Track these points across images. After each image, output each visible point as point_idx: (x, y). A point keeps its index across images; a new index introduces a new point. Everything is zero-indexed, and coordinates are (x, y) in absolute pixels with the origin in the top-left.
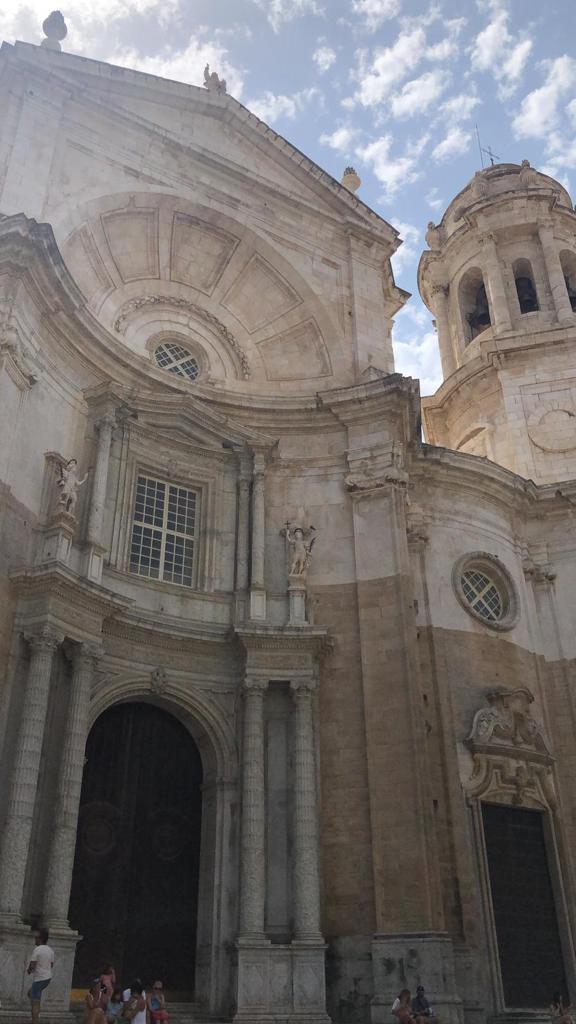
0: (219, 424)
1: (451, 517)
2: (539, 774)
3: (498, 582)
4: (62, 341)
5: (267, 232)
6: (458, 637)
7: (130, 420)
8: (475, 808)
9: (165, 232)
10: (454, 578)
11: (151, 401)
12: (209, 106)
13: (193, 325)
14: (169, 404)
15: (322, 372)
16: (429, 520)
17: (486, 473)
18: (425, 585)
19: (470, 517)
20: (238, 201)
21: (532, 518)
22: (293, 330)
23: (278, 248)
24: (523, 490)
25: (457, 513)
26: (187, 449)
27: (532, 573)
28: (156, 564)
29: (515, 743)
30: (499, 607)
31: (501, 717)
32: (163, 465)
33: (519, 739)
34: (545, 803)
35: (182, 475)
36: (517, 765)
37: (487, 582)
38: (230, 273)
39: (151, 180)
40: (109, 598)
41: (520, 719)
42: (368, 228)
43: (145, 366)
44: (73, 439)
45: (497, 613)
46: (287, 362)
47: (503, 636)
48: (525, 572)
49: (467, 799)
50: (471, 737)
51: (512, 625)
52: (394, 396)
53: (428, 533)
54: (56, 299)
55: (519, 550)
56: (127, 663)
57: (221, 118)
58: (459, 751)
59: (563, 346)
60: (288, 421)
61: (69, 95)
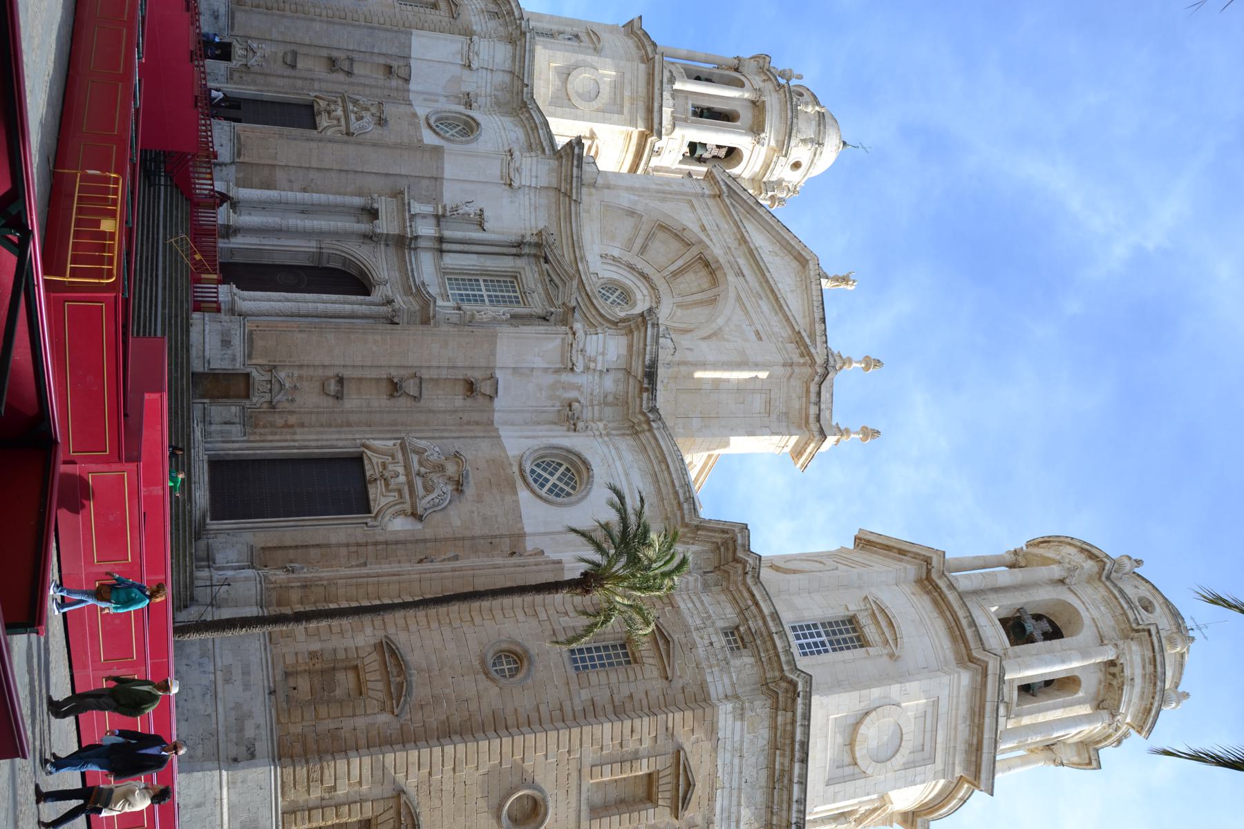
4: (558, 213)
7: (542, 260)
11: (558, 260)
14: (565, 271)
19: (620, 459)
20: (744, 276)
39: (708, 236)
40: (408, 224)
42: (809, 343)
43: (581, 259)
47: (520, 483)
54: (568, 187)
56: (385, 266)
61: (718, 193)
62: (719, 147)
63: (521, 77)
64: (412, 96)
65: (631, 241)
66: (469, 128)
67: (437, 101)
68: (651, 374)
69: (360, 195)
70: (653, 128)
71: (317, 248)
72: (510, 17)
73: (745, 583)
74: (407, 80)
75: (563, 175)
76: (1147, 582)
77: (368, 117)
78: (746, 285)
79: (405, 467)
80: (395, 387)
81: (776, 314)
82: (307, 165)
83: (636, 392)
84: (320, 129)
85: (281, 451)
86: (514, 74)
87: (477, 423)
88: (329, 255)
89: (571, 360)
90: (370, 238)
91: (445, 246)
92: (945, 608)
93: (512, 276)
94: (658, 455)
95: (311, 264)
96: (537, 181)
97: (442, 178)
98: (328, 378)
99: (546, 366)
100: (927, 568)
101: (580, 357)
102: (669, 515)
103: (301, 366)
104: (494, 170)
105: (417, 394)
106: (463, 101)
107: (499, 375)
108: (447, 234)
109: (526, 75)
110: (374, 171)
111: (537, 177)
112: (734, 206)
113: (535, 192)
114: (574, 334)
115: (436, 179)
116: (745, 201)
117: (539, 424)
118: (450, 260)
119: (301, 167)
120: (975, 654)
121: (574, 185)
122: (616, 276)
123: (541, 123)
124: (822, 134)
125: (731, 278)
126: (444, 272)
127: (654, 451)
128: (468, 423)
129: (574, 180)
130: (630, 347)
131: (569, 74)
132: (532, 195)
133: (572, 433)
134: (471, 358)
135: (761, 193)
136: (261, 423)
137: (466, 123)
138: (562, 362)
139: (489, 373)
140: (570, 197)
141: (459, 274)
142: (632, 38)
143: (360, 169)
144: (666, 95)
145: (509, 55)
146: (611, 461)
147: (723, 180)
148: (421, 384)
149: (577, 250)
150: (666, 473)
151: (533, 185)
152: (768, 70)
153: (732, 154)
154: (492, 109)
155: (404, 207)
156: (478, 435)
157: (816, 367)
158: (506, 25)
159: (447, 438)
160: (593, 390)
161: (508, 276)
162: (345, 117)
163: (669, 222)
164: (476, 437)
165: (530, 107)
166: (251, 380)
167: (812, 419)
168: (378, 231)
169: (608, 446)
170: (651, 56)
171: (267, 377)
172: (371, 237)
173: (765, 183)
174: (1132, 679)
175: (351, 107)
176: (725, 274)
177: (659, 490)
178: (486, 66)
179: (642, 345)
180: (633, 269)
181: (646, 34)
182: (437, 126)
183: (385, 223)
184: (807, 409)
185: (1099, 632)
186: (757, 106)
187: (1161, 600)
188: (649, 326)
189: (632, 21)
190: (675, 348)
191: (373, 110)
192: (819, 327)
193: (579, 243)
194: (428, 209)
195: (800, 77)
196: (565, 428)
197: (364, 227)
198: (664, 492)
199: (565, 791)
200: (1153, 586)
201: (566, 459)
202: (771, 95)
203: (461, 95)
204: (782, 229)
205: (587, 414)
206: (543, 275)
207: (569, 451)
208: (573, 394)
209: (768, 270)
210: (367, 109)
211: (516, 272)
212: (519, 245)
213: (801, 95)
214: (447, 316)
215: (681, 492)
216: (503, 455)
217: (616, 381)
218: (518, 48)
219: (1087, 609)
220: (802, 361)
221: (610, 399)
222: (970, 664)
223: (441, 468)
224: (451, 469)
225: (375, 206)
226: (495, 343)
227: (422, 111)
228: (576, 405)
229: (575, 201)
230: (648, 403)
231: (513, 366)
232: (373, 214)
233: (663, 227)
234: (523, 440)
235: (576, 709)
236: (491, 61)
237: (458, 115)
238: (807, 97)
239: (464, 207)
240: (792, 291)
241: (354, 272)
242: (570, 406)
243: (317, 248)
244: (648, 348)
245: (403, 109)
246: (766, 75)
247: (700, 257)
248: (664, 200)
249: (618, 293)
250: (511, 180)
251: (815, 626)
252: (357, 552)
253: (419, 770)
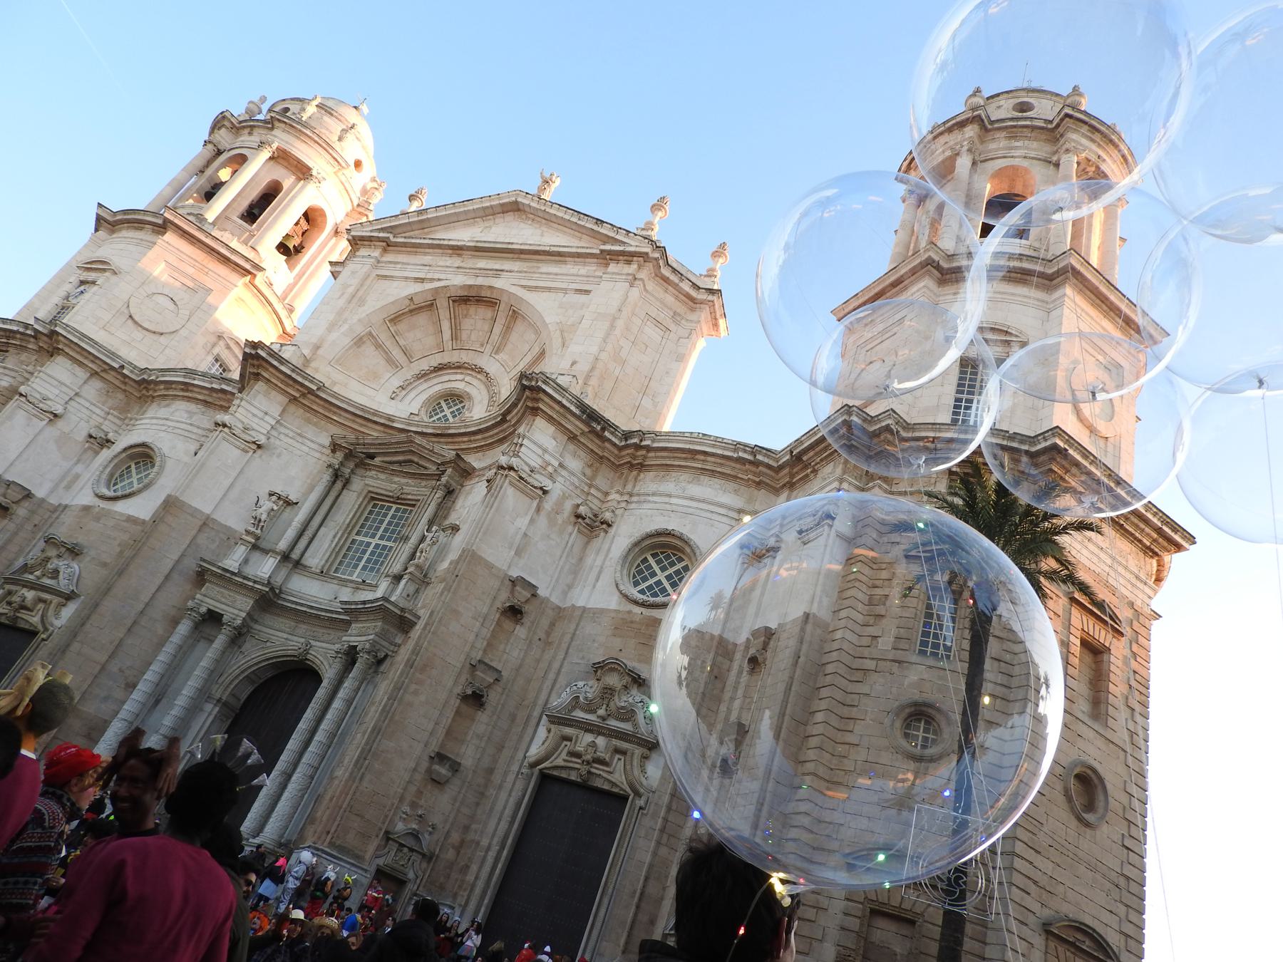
0: (431, 451)
9: (444, 314)
11: (380, 444)
12: (502, 205)
13: (468, 379)
14: (397, 443)
17: (692, 447)
19: (670, 496)
26: (413, 475)
28: (356, 566)
32: (391, 491)
35: (403, 496)
38: (498, 329)
39: (432, 280)
40: (251, 584)
42: (621, 248)
43: (389, 419)
44: (309, 481)
57: (519, 210)
62: (297, 224)
63: (107, 367)
64: (53, 500)
65: (391, 361)
66: (142, 456)
67: (77, 477)
68: (591, 416)
69: (175, 622)
70: (248, 270)
71: (215, 705)
72: (14, 338)
73: (906, 440)
74: (28, 495)
75: (280, 385)
76: (998, 95)
77: (61, 564)
78: (513, 274)
79: (587, 731)
80: (475, 699)
81: (565, 262)
82: (99, 667)
83: (597, 441)
84: (40, 628)
85: (498, 871)
86: (96, 373)
87: (552, 625)
88: (233, 695)
89: (535, 487)
90: (239, 636)
91: (295, 555)
93: (369, 502)
94: (684, 456)
95: (230, 721)
96: (271, 416)
97: (208, 517)
98: (429, 771)
99: (528, 518)
100: (935, 267)
101: (537, 476)
102: (757, 480)
103: (402, 799)
104: (230, 453)
105: (495, 676)
106: (96, 447)
107: (514, 573)
108: (283, 545)
109: (108, 361)
110: (153, 590)
111: (266, 414)
112: (409, 237)
113: (281, 425)
114: (511, 468)
115: (204, 524)
116: (409, 223)
117: (581, 559)
118: (315, 559)
119: (96, 677)
120: (1050, 271)
121: (300, 379)
122: (424, 396)
123: (184, 377)
124: (342, 118)
125: (499, 283)
126: (323, 574)
128: (548, 634)
129: (294, 375)
130: (550, 419)
131: (131, 316)
132: (282, 430)
133: (612, 531)
134: (483, 593)
135: (367, 216)
136: (442, 879)
137: (131, 457)
138: (532, 498)
139: (507, 582)
140: (311, 392)
141: (336, 557)
142: (120, 230)
143: (142, 606)
144: (216, 233)
145: (68, 363)
146: (668, 507)
147: (371, 231)
148: (486, 664)
149: (375, 419)
150: (709, 459)
151: (273, 422)
152: (241, 122)
153: (311, 218)
154: (126, 421)
155: (227, 579)
156: (571, 630)
157: (651, 255)
158: (23, 348)
159: (561, 666)
160: (573, 484)
161: (366, 506)
162: (42, 591)
163: (394, 310)
164: (574, 634)
165: (153, 378)
166: (388, 870)
167: (693, 293)
168: (239, 622)
170: (160, 221)
171: (394, 847)
172: (240, 634)
173: (358, 205)
174: (1099, 157)
175: (31, 577)
176: (491, 287)
177: (724, 475)
178: (67, 398)
179: (557, 407)
180: (425, 375)
181: (125, 212)
182: (115, 491)
183: (231, 610)
184: (680, 291)
185: (1040, 159)
186: (282, 157)
187: (1024, 94)
188: (544, 387)
189: (99, 219)
190: (574, 376)
191: (52, 552)
192: (604, 230)
193: (369, 412)
194: (240, 552)
195: (263, 99)
196: (602, 534)
197: (221, 640)
198: (728, 472)
199: (1079, 738)
200: (1007, 92)
201: (642, 551)
202: (275, 136)
203: (87, 445)
204: (464, 206)
205: (595, 504)
206: (386, 469)
207: (636, 544)
208: (568, 506)
209: (509, 243)
210: (47, 559)
211: (366, 496)
212: (336, 475)
213: (287, 110)
214: (404, 595)
215: (741, 454)
216: (613, 615)
217: (574, 455)
218: (67, 350)
219: (1012, 157)
220: (634, 266)
221: (588, 472)
222: (1055, 282)
223: (608, 692)
224: (613, 680)
225: (203, 610)
226: (480, 557)
227: (84, 497)
228: (582, 510)
229: (318, 389)
230: (616, 436)
231: (513, 553)
232: (213, 618)
233: (396, 319)
234: (599, 584)
235: (999, 682)
236: (64, 389)
237: (116, 461)
238: (294, 108)
239: (261, 510)
240: (542, 235)
241: (269, 675)
242: (578, 516)
243: (215, 705)
244: (564, 402)
245: (68, 519)
246: (244, 127)
247: (453, 301)
248: (362, 302)
249: (443, 404)
250: (254, 443)
251: (957, 400)
252: (670, 835)
253: (1029, 894)
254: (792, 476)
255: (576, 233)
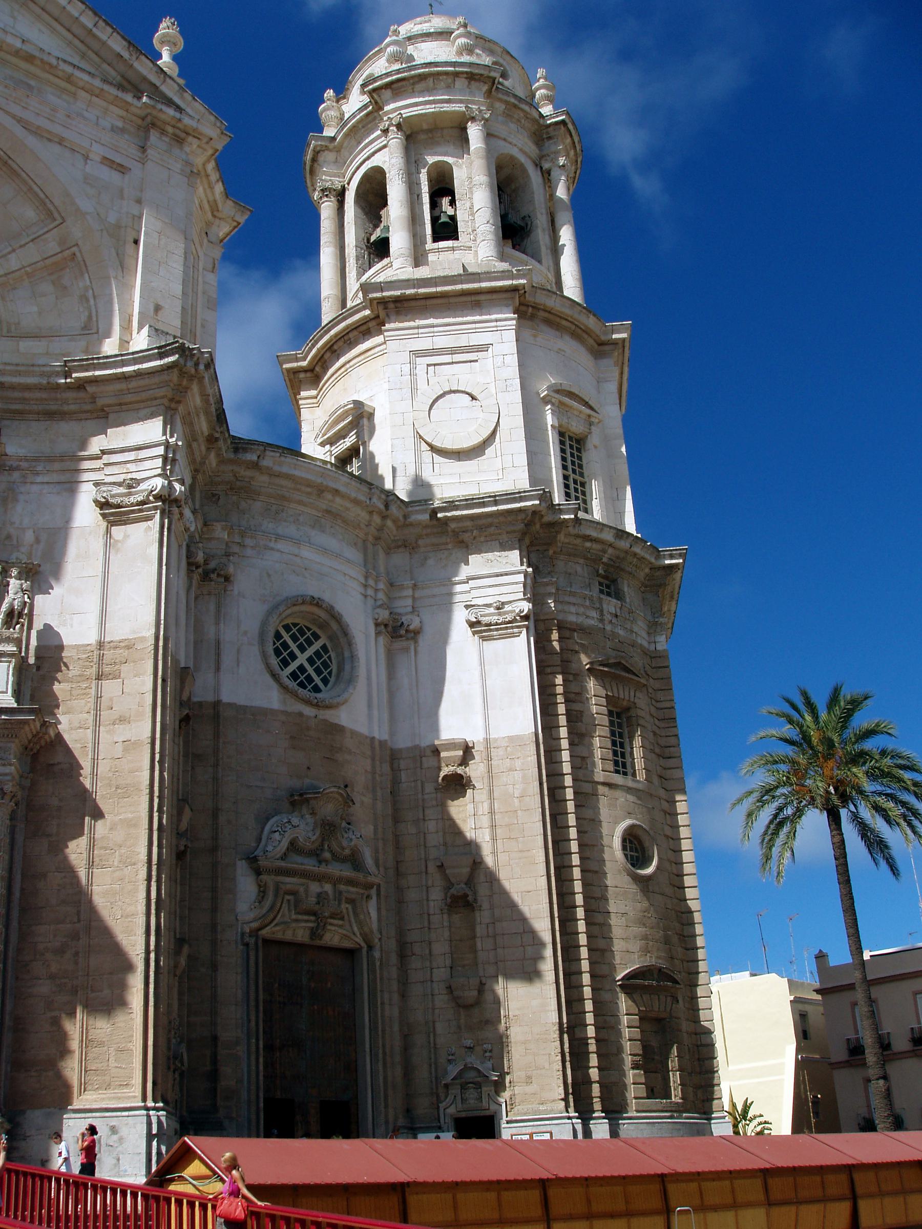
1: (272, 545)
2: (352, 901)
3: (331, 638)
5: (14, 117)
6: (256, 716)
8: (252, 946)
10: (262, 635)
15: (83, 329)
16: (235, 549)
18: (218, 643)
21: (398, 547)
22: (48, 262)
23: (31, 141)
24: (382, 507)
25: (279, 537)
27: (386, 626)
29: (320, 862)
30: (330, 673)
31: (302, 826)
33: (327, 855)
34: (359, 940)
36: (319, 890)
37: (317, 637)
41: (329, 829)
45: (325, 681)
46: (35, 309)
48: (377, 625)
49: (243, 934)
50: (256, 853)
51: (335, 701)
52: (174, 376)
53: (231, 569)
55: (370, 592)
58: (239, 871)
59: (473, 298)
60: (24, 400)
92: (558, 320)
127: (298, 490)
169: (267, 548)
254: (420, 537)
255: (77, 42)
